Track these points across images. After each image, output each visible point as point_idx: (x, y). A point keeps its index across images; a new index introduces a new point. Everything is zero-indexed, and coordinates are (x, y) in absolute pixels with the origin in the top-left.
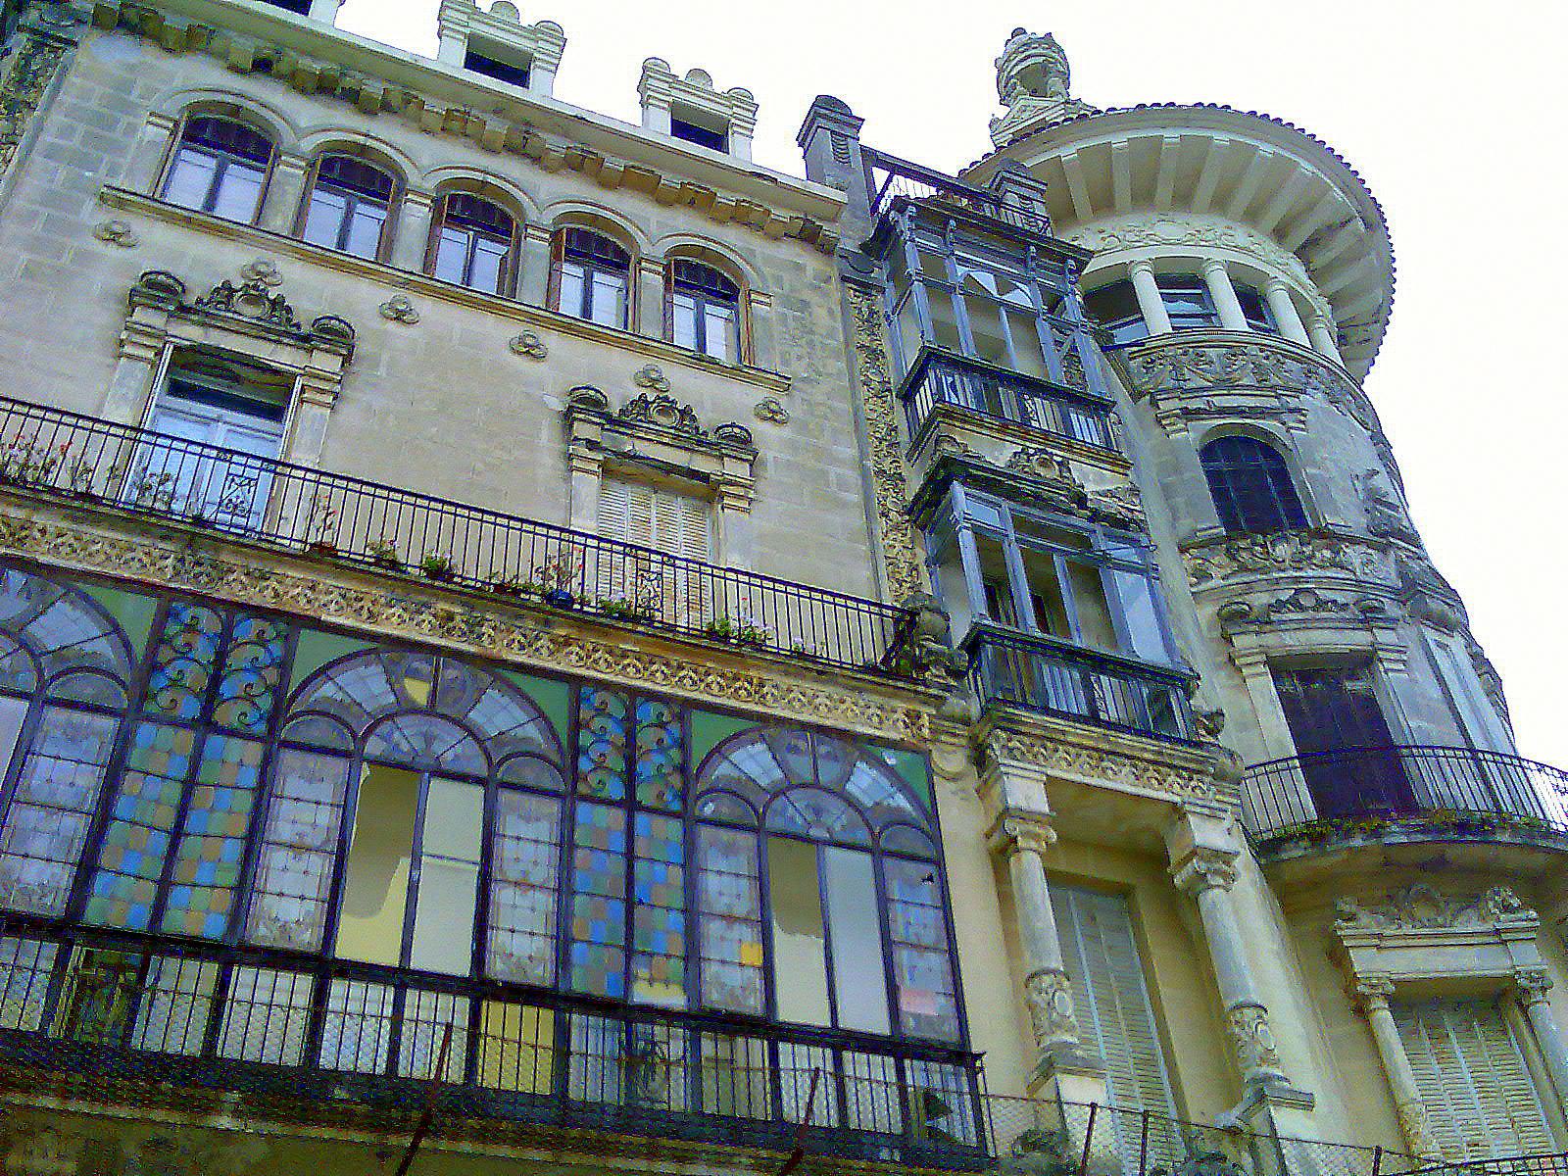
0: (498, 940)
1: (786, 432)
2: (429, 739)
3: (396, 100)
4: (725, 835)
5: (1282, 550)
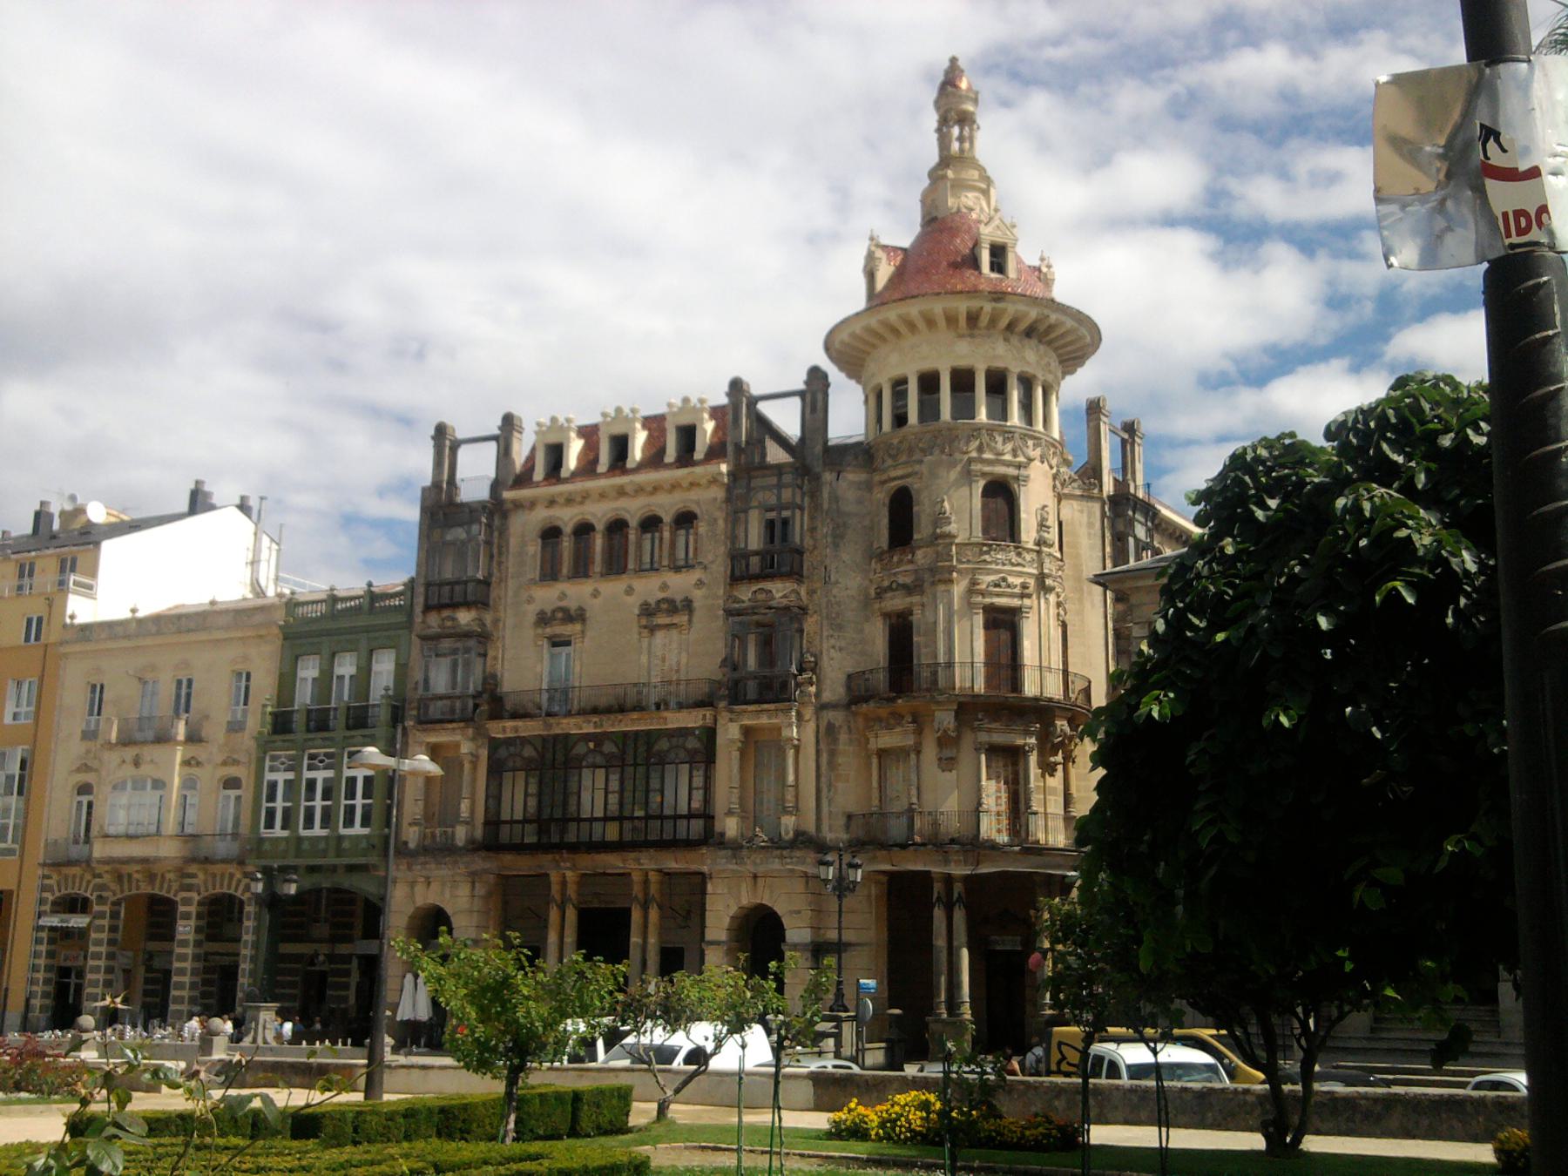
0: (609, 807)
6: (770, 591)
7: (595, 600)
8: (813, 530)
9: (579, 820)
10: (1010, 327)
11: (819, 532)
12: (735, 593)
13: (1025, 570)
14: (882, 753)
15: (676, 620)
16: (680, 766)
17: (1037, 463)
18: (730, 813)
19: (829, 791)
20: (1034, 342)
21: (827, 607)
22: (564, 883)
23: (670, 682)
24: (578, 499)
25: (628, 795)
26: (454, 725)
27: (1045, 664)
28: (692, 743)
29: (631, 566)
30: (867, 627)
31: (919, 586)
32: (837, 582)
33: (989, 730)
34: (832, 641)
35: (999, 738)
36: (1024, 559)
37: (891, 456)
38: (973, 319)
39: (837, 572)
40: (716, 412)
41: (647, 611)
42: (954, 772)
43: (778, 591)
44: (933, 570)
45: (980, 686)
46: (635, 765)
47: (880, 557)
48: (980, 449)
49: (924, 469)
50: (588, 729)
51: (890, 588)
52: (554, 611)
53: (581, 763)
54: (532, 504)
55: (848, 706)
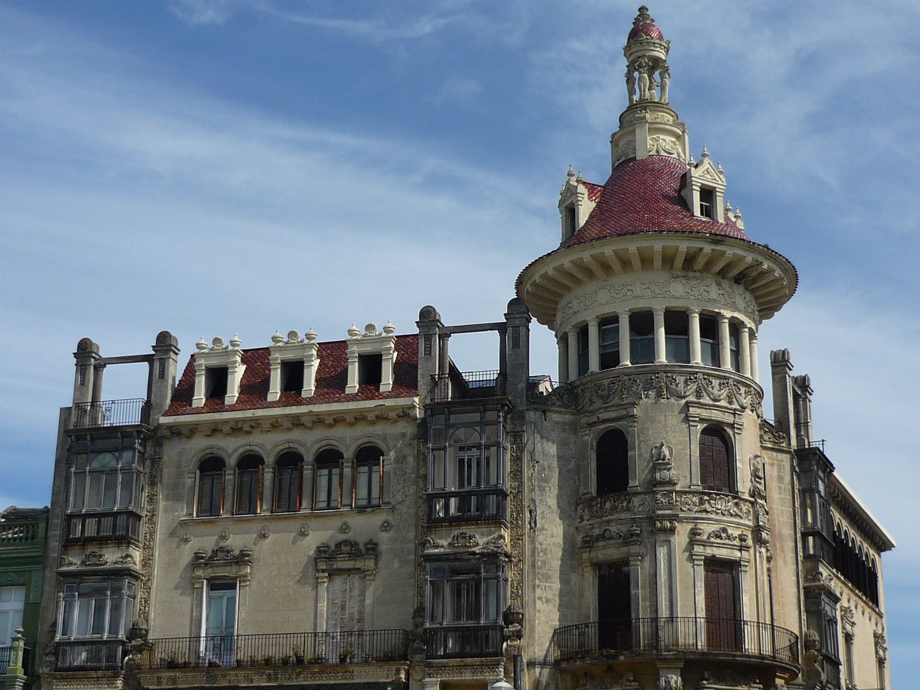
1: (391, 534)
3: (253, 424)
10: (722, 273)
13: (742, 521)
15: (359, 564)
17: (748, 411)
20: (741, 289)
23: (351, 633)
24: (247, 428)
26: (100, 673)
27: (761, 621)
32: (543, 529)
36: (741, 510)
37: (602, 397)
38: (690, 260)
39: (543, 518)
40: (404, 342)
45: (702, 644)
47: (589, 503)
51: (602, 537)
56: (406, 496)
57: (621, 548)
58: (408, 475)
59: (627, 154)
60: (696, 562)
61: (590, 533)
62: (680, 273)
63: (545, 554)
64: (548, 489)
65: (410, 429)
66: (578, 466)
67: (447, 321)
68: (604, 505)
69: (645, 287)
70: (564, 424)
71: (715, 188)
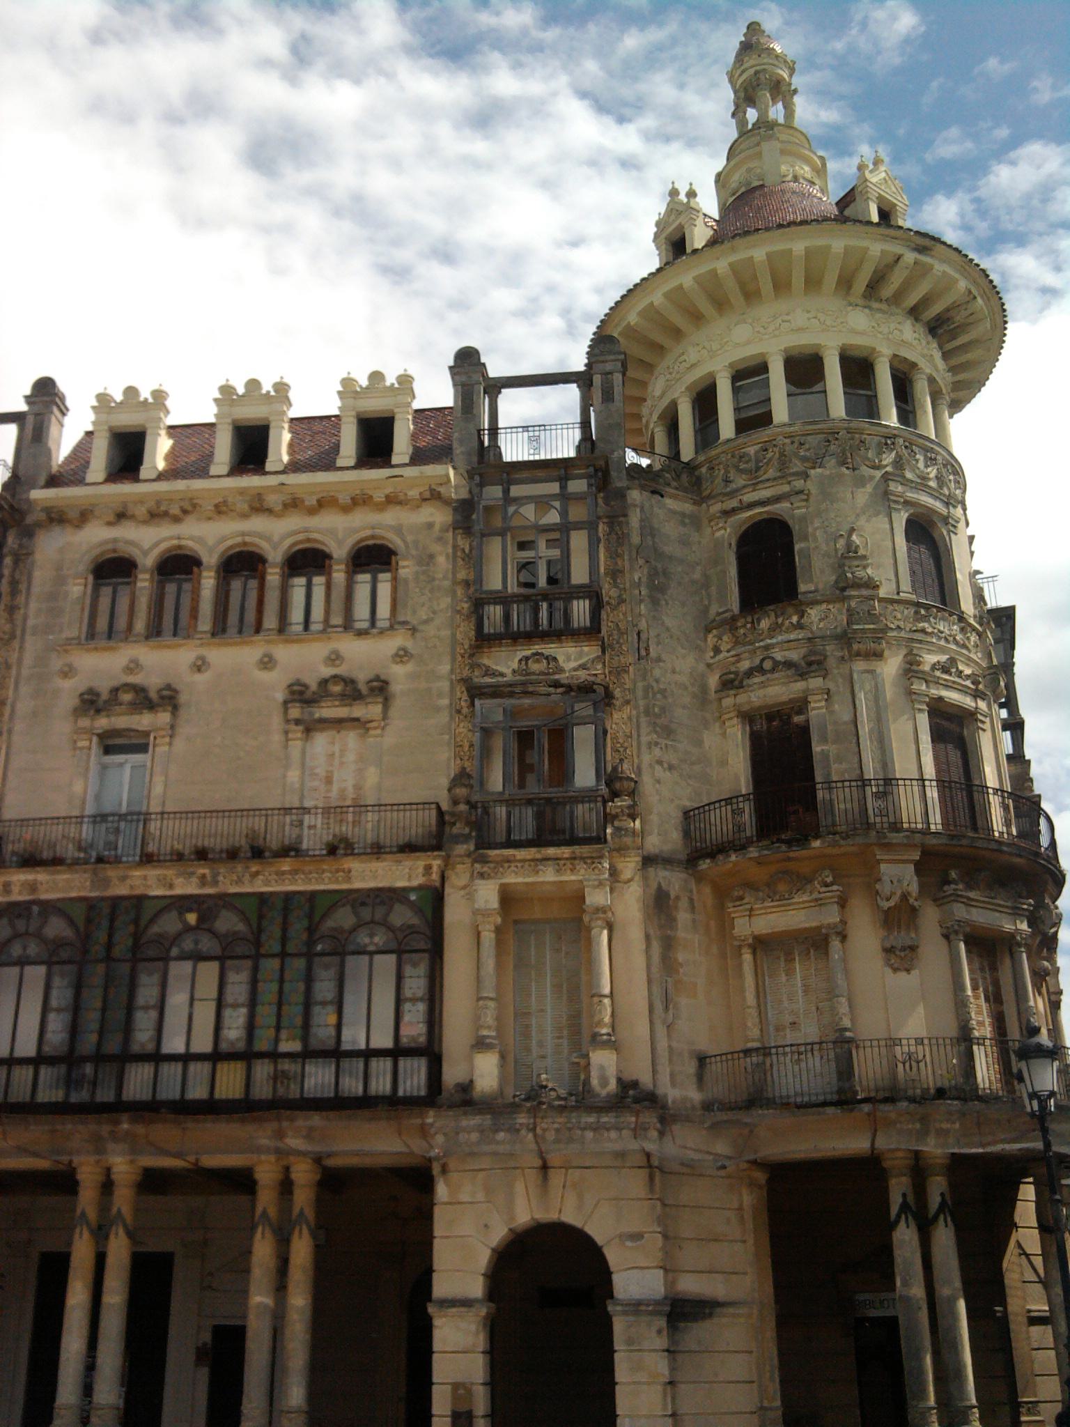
1: (410, 667)
2: (196, 942)
3: (188, 507)
4: (327, 959)
5: (765, 624)
6: (555, 659)
7: (198, 678)
8: (615, 574)
9: (157, 1058)
11: (627, 575)
12: (486, 661)
14: (762, 944)
15: (358, 711)
16: (377, 958)
18: (481, 1044)
19: (667, 1008)
21: (645, 697)
22: (107, 1186)
25: (266, 1013)
28: (401, 916)
29: (270, 621)
30: (711, 739)
31: (819, 663)
32: (659, 660)
33: (969, 903)
34: (657, 752)
35: (982, 917)
36: (968, 638)
41: (299, 695)
42: (915, 973)
43: (569, 659)
44: (845, 638)
46: (283, 955)
47: (730, 624)
48: (898, 463)
49: (811, 486)
50: (186, 886)
52: (115, 691)
53: (168, 950)
54: (84, 516)
55: (691, 861)
56: (434, 612)
57: (792, 684)
58: (437, 582)
59: (750, 183)
60: (917, 706)
61: (733, 669)
62: (860, 302)
63: (665, 697)
64: (664, 603)
65: (439, 516)
66: (705, 576)
67: (496, 368)
68: (759, 625)
69: (810, 315)
70: (683, 515)
71: (896, 205)
